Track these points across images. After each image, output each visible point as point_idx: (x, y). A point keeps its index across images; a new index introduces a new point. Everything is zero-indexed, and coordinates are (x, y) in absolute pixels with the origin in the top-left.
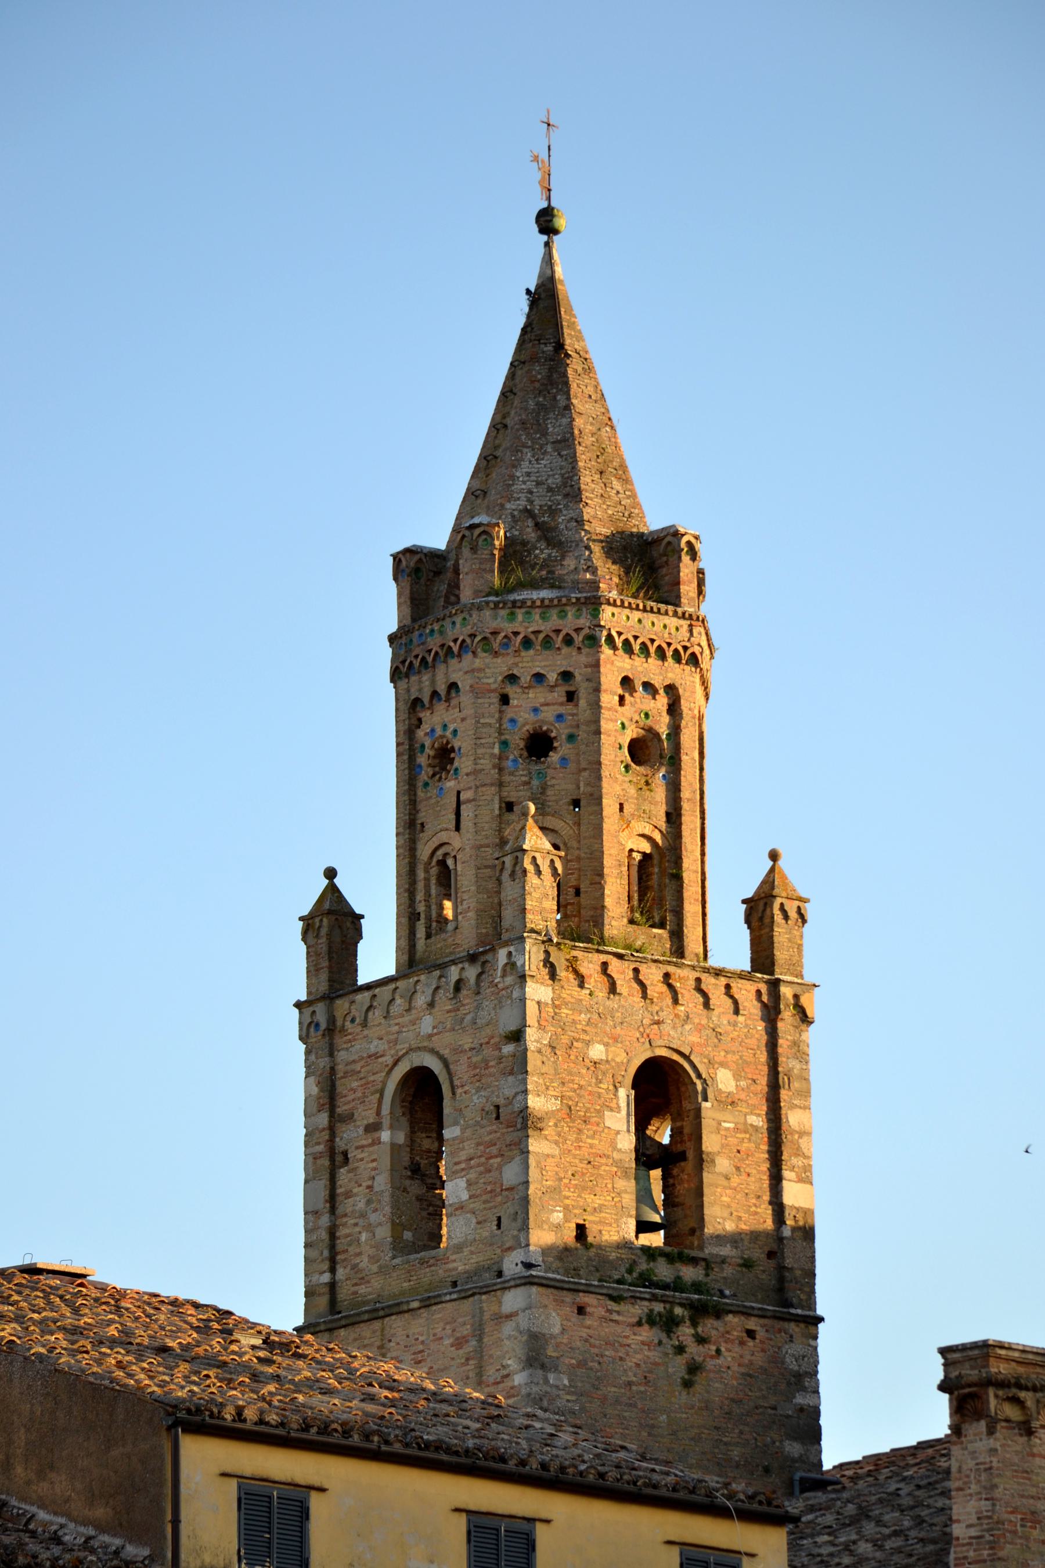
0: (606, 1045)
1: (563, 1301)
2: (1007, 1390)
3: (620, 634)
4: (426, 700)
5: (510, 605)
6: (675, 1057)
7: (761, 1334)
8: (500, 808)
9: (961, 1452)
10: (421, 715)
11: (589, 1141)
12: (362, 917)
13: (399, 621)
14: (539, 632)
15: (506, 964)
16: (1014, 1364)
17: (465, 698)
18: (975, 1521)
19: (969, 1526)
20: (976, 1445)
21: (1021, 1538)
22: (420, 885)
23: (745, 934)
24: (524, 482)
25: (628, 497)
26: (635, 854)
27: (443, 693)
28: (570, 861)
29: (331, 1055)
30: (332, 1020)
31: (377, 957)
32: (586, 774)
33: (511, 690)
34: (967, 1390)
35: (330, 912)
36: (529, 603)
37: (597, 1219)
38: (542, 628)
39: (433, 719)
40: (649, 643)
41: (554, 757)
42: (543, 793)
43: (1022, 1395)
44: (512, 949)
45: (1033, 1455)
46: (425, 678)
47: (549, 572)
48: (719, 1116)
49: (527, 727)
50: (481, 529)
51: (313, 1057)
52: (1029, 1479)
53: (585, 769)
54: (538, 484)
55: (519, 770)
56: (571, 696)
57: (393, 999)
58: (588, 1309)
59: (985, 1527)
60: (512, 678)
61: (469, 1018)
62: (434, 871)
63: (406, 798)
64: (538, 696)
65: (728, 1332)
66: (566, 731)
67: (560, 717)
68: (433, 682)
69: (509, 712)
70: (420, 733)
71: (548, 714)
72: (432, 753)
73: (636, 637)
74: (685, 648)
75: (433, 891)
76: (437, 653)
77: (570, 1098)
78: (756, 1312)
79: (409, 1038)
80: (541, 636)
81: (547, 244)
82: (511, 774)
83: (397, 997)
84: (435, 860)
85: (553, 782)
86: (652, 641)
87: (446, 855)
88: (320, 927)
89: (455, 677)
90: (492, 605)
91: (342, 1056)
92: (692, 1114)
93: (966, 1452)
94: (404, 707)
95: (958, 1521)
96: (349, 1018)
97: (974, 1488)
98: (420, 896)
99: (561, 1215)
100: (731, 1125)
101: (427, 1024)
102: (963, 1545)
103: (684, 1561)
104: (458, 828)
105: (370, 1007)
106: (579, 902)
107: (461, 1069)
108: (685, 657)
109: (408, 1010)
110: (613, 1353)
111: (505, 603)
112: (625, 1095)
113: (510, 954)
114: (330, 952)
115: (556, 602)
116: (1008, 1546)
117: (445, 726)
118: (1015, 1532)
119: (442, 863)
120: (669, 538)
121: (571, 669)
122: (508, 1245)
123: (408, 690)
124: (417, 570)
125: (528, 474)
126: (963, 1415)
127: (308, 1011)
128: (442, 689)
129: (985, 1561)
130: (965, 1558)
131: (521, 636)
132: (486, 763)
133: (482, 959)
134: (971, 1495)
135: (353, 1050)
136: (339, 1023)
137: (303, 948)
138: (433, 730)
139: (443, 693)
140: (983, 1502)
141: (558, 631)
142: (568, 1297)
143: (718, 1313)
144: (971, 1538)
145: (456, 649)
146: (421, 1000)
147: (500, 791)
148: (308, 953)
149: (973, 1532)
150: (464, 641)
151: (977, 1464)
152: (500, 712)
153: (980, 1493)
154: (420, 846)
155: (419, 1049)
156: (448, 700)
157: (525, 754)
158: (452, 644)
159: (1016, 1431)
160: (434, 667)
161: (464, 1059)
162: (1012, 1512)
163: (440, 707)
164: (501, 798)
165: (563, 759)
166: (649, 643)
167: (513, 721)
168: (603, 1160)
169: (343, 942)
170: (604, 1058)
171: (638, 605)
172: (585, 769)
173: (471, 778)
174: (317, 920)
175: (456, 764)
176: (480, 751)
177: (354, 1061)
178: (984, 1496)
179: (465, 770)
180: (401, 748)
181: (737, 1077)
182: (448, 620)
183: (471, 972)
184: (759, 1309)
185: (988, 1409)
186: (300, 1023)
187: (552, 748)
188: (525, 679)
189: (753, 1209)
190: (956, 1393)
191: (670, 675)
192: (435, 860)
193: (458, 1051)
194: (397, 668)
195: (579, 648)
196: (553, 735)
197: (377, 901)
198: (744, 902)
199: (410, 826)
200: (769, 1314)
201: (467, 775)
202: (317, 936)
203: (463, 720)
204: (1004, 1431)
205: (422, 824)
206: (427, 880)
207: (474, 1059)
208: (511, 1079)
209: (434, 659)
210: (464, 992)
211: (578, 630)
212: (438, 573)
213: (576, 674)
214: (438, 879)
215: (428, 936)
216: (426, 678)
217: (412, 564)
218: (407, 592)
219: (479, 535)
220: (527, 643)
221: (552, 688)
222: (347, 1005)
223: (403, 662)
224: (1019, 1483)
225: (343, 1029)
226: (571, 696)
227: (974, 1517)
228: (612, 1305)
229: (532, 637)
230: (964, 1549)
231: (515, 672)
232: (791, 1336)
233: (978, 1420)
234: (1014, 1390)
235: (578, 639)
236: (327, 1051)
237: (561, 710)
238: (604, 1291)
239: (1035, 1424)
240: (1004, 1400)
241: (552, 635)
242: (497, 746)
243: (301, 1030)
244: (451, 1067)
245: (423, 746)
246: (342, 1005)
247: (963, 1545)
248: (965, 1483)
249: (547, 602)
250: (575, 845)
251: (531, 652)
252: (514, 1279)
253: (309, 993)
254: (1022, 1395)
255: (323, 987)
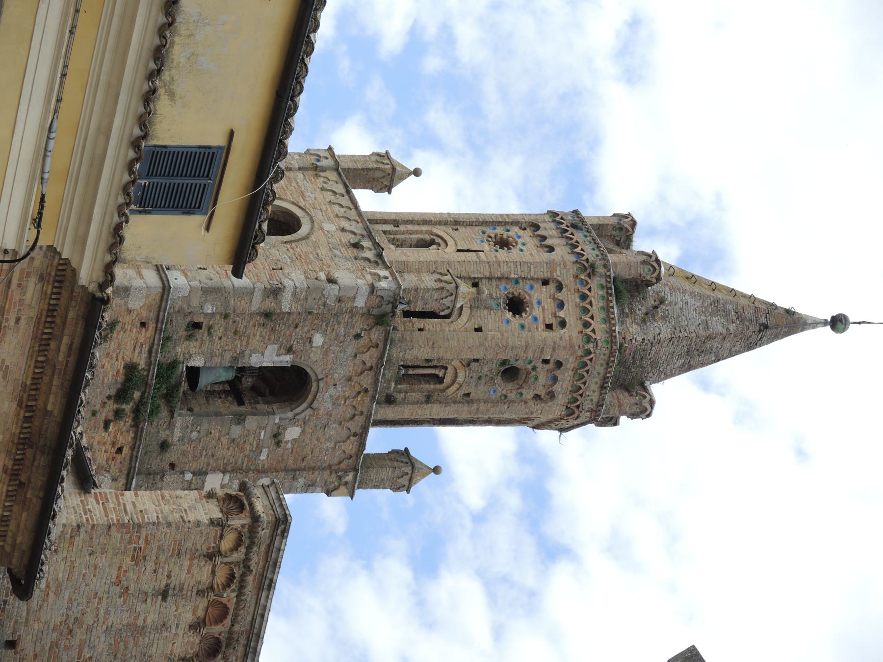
0: (322, 346)
1: (150, 311)
2: (248, 535)
3: (591, 360)
4: (539, 232)
5: (609, 285)
6: (310, 397)
7: (119, 457)
8: (475, 278)
9: (193, 498)
10: (528, 229)
11: (258, 333)
12: (390, 192)
13: (587, 217)
14: (591, 305)
15: (379, 276)
16: (268, 541)
17: (545, 256)
18: (140, 507)
19: (133, 503)
20: (201, 510)
21: (125, 548)
22: (417, 228)
23: (385, 450)
24: (682, 300)
25: (671, 371)
26: (443, 371)
27: (546, 242)
28: (441, 325)
29: (300, 169)
30: (324, 170)
31: (368, 200)
32: (499, 336)
33: (552, 287)
34: (245, 502)
35: (394, 169)
36: (610, 298)
37: (204, 338)
38: (594, 308)
39: (526, 236)
40: (583, 381)
41: (509, 315)
42: (485, 308)
43: (243, 549)
44: (390, 279)
45: (191, 559)
46: (554, 232)
47: (627, 314)
48: (269, 429)
49: (527, 297)
50: (657, 267)
51: (297, 157)
52: (172, 556)
53: (502, 335)
54: (681, 309)
55: (502, 291)
56: (549, 327)
57: (343, 207)
58: (144, 330)
59: (135, 516)
60: (560, 287)
61: (338, 253)
62: (428, 237)
63: (474, 220)
64: (550, 305)
65: (122, 433)
66: (526, 324)
67: (536, 319)
68: (551, 237)
69: (538, 285)
70: (516, 229)
71: (537, 312)
72: (505, 236)
73: (587, 372)
74: (578, 407)
75: (413, 236)
76: (572, 239)
77: (288, 320)
78: (135, 453)
79: (319, 216)
80: (589, 307)
81: (825, 323)
82: (497, 287)
83: (344, 209)
84: (434, 237)
85: (493, 314)
86: (585, 383)
87: (439, 245)
88: (383, 163)
89: (558, 250)
90: (608, 274)
91: (300, 175)
92: (270, 409)
93: (194, 502)
94: (533, 218)
95: (136, 495)
96: (325, 180)
97: (166, 509)
98: (410, 227)
99: (210, 311)
100: (262, 437)
101: (329, 227)
102: (118, 499)
103: (211, 151)
104: (459, 251)
105: (335, 193)
106: (414, 331)
107: (302, 247)
108: (572, 406)
109: (337, 216)
110: (112, 348)
111: (609, 282)
112: (286, 360)
113: (386, 278)
114: (368, 170)
115: (612, 316)
116: (120, 535)
117: (524, 244)
118: (130, 542)
119: (432, 243)
120: (648, 397)
121: (567, 327)
122: (189, 274)
123: (545, 222)
124: (621, 229)
125: (687, 303)
126: (224, 500)
127: (327, 154)
128: (548, 242)
129: (107, 516)
130: (107, 501)
131: (588, 293)
132: (504, 269)
133: (380, 262)
134: (160, 505)
135: (305, 182)
136: (322, 174)
137: (368, 153)
138: (519, 237)
139: (546, 242)
140: (155, 515)
141: (592, 317)
142: (152, 315)
144: (124, 505)
145: (578, 250)
146: (345, 224)
147: (485, 278)
148: (365, 156)
149: (129, 507)
150: (583, 255)
151: (185, 510)
152: (538, 279)
153: (162, 512)
154: (443, 227)
155: (313, 222)
156: (542, 246)
157: (511, 296)
158: (580, 248)
159: (213, 545)
160: (562, 237)
161: (310, 249)
162: (146, 540)
163: (536, 241)
164: (481, 278)
165: (508, 321)
166: (583, 381)
167: (532, 287)
168: (244, 344)
169: (374, 179)
170: (314, 345)
171: (610, 372)
172: (502, 335)
173: (494, 259)
174: (388, 162)
175: (500, 250)
176: (512, 266)
177: (297, 183)
178: (160, 516)
179: (499, 256)
180: (506, 217)
181: (295, 441)
182: (595, 246)
183: (370, 254)
184: (137, 457)
185: (233, 519)
186: (319, 150)
187: (514, 314)
188: (560, 296)
189: (205, 453)
190: (242, 494)
191: (561, 396)
192: (434, 237)
193: (316, 246)
194: (558, 215)
195: (582, 332)
196: (524, 314)
197: (403, 200)
198: (406, 449)
199: (456, 222)
200: (133, 463)
201: (496, 257)
202: (377, 162)
203: (531, 254)
204: (213, 534)
205: (457, 229)
206: (421, 232)
207: (311, 256)
208: (303, 277)
209: (567, 237)
210: (355, 250)
211: (593, 331)
212: (618, 244)
213: (564, 330)
214: (422, 240)
215: (385, 232)
216: (554, 233)
217: (626, 225)
218: (607, 222)
219: (653, 266)
220: (584, 297)
221: (555, 315)
222: (334, 179)
223: (562, 218)
224: (169, 546)
225: (317, 176)
226: (549, 327)
227: (142, 508)
228: (146, 348)
229: (588, 301)
230: (115, 500)
231: (564, 289)
232: (116, 480)
233: (222, 511)
234: (247, 542)
235: (588, 331)
236: (302, 166)
237: (540, 320)
238: (156, 342)
239: (219, 560)
240: (240, 533)
241: (590, 315)
242: (516, 276)
243: (314, 150)
244: (304, 241)
245: (508, 231)
246: (333, 176)
247: (118, 499)
248: (168, 501)
249: (611, 310)
250: (452, 329)
251: (578, 300)
252: (166, 276)
253: (339, 156)
254: (243, 549)
255: (344, 165)
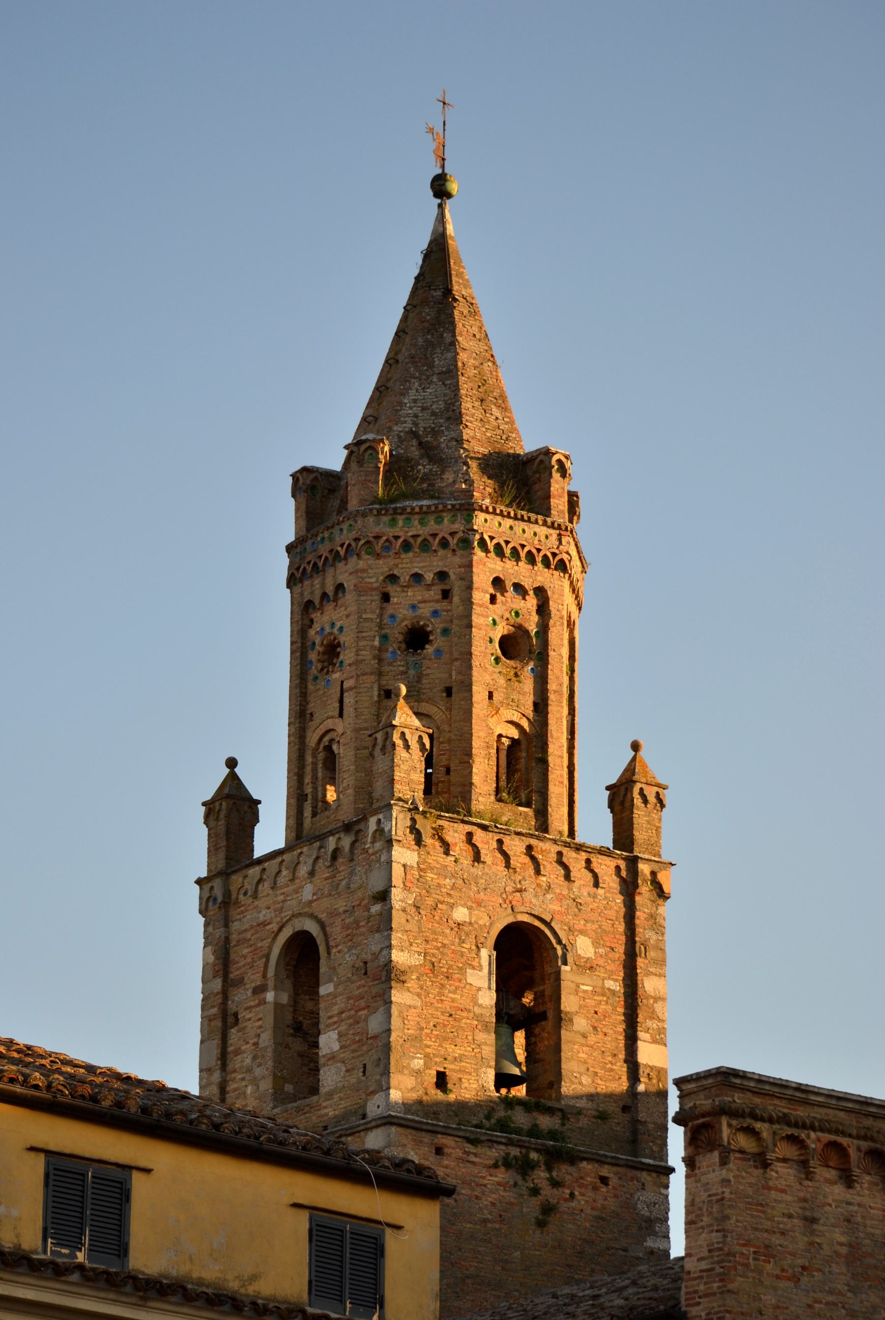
0: (470, 908)
1: (421, 1142)
2: (741, 1120)
3: (492, 538)
4: (317, 602)
5: (391, 511)
6: (537, 923)
7: (614, 1181)
8: (379, 695)
10: (313, 616)
11: (451, 995)
12: (259, 802)
13: (296, 533)
14: (418, 536)
15: (376, 831)
16: (749, 1095)
17: (349, 597)
18: (705, 1253)
19: (699, 1260)
21: (753, 1271)
22: (308, 769)
23: (608, 817)
24: (411, 408)
25: (507, 423)
26: (504, 740)
28: (442, 743)
29: (226, 925)
30: (227, 893)
31: (270, 834)
32: (457, 664)
33: (392, 589)
34: (701, 1121)
35: (228, 796)
36: (409, 510)
37: (457, 1068)
38: (421, 532)
39: (322, 620)
40: (519, 548)
41: (430, 649)
42: (419, 681)
43: (758, 1125)
44: (381, 816)
45: (769, 1188)
46: (316, 581)
47: (429, 485)
48: (578, 979)
49: (406, 623)
50: (367, 444)
51: (210, 929)
52: (764, 1212)
54: (424, 409)
56: (446, 594)
57: (280, 871)
58: (446, 1150)
59: (716, 1259)
60: (392, 578)
61: (344, 883)
62: (321, 756)
63: (298, 691)
64: (415, 594)
65: (582, 1178)
66: (441, 626)
67: (435, 613)
68: (323, 585)
69: (390, 609)
70: (312, 632)
71: (425, 610)
72: (321, 649)
73: (507, 542)
74: (554, 555)
75: (320, 775)
76: (326, 558)
77: (434, 955)
78: (609, 1160)
79: (292, 905)
80: (420, 540)
81: (441, 206)
83: (283, 869)
84: (322, 746)
85: (429, 671)
86: (523, 546)
87: (332, 741)
88: (219, 810)
89: (342, 578)
90: (375, 512)
91: (235, 926)
92: (553, 977)
93: (699, 1185)
94: (297, 609)
96: (242, 892)
97: (706, 1220)
98: (308, 779)
99: (421, 1062)
100: (589, 988)
101: (308, 892)
102: (695, 1279)
104: (341, 715)
105: (260, 880)
106: (449, 781)
107: (336, 931)
109: (292, 880)
110: (469, 1192)
111: (387, 510)
112: (487, 955)
113: (379, 821)
114: (228, 832)
115: (433, 508)
116: (738, 1278)
117: (333, 625)
118: (747, 1265)
119: (328, 749)
120: (541, 457)
121: (446, 569)
122: (371, 1089)
123: (302, 594)
125: (415, 401)
126: (697, 1147)
127: (207, 887)
128: (330, 590)
129: (714, 1294)
130: (696, 1292)
131: (401, 540)
132: (366, 654)
133: (356, 828)
134: (703, 1228)
135: (245, 920)
136: (234, 896)
137: (205, 830)
138: (323, 629)
140: (714, 1234)
141: (434, 535)
142: (427, 1138)
143: (573, 1159)
144: (701, 1271)
145: (342, 553)
146: (303, 870)
147: (379, 680)
148: (209, 835)
149: (704, 1265)
150: (349, 545)
151: (709, 1196)
152: (382, 608)
153: (711, 1225)
154: (309, 734)
155: (300, 915)
156: (336, 600)
157: (403, 646)
158: (339, 549)
159: (751, 1163)
160: (324, 571)
161: (338, 921)
162: (744, 1245)
163: (329, 607)
164: (380, 686)
165: (438, 651)
166: (519, 548)
167: (393, 616)
168: (465, 1014)
169: (240, 824)
170: (468, 920)
171: (509, 513)
172: (456, 659)
173: (354, 668)
174: (217, 804)
175: (341, 657)
176: (361, 643)
177: (246, 930)
178: (715, 1228)
179: (348, 662)
180: (295, 646)
181: (596, 944)
182: (337, 528)
183: (346, 842)
184: (612, 1157)
185: (721, 1138)
186: (200, 898)
187: (428, 642)
188: (405, 578)
189: (609, 1066)
190: (690, 1124)
191: (539, 578)
192: (322, 746)
193: (333, 914)
195: (454, 550)
196: (429, 629)
197: (270, 786)
198: (608, 788)
200: (622, 1162)
201: (350, 665)
202: (217, 819)
203: (348, 616)
204: (739, 1162)
205: (311, 714)
206: (314, 764)
207: (347, 921)
208: (377, 935)
209: (324, 564)
210: (340, 860)
211: (452, 534)
212: (332, 491)
213: (451, 574)
214: (324, 764)
215: (314, 814)
216: (317, 582)
217: (308, 482)
218: (303, 506)
219: (366, 450)
220: (407, 546)
221: (429, 586)
222: (240, 880)
224: (752, 1216)
225: (237, 903)
226: (446, 594)
227: (705, 1249)
228: (469, 1148)
229: (411, 540)
230: (695, 1282)
231: (395, 572)
232: (643, 1184)
233: (711, 1151)
235: (453, 542)
236: (222, 922)
237: (437, 606)
238: (461, 1134)
239: (770, 1156)
240: (738, 1130)
241: (430, 539)
242: (377, 638)
243: (200, 904)
244: (328, 929)
245: (314, 644)
246: (236, 880)
247: (695, 1279)
248: (697, 1216)
249: (425, 509)
250: (447, 728)
251: (411, 554)
252: (375, 1120)
253: (209, 871)
254: (758, 1125)
255: (221, 865)
